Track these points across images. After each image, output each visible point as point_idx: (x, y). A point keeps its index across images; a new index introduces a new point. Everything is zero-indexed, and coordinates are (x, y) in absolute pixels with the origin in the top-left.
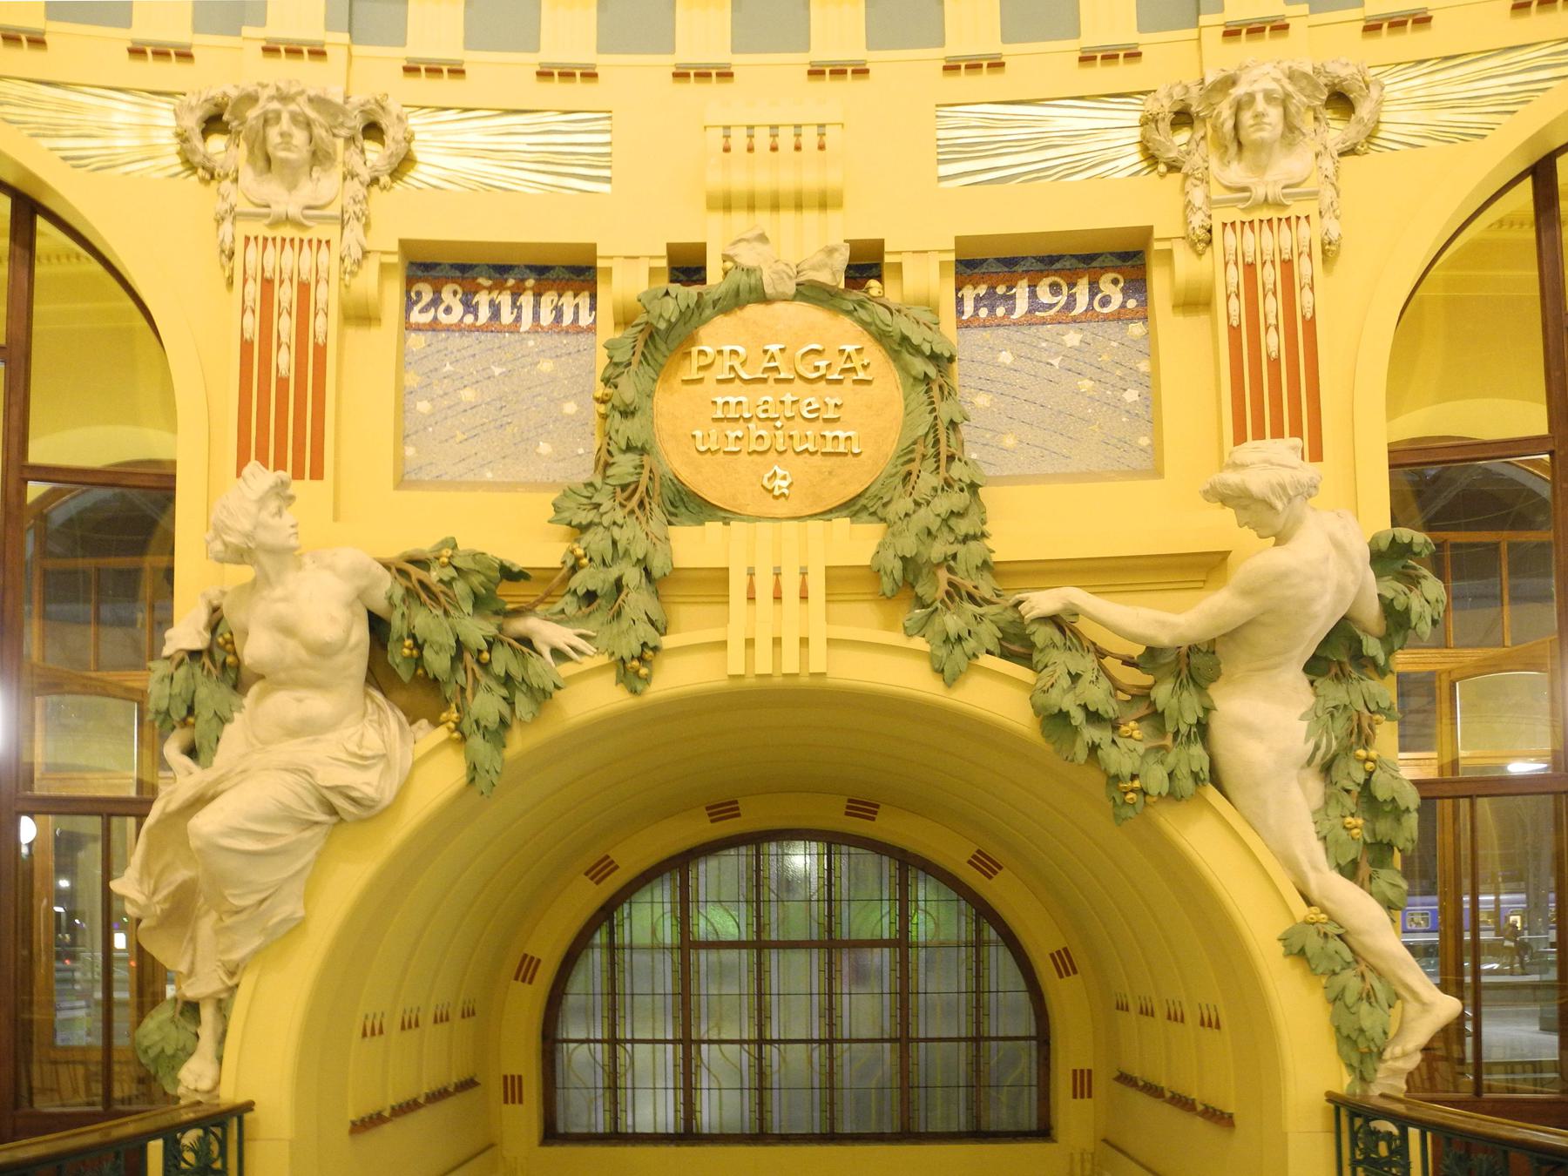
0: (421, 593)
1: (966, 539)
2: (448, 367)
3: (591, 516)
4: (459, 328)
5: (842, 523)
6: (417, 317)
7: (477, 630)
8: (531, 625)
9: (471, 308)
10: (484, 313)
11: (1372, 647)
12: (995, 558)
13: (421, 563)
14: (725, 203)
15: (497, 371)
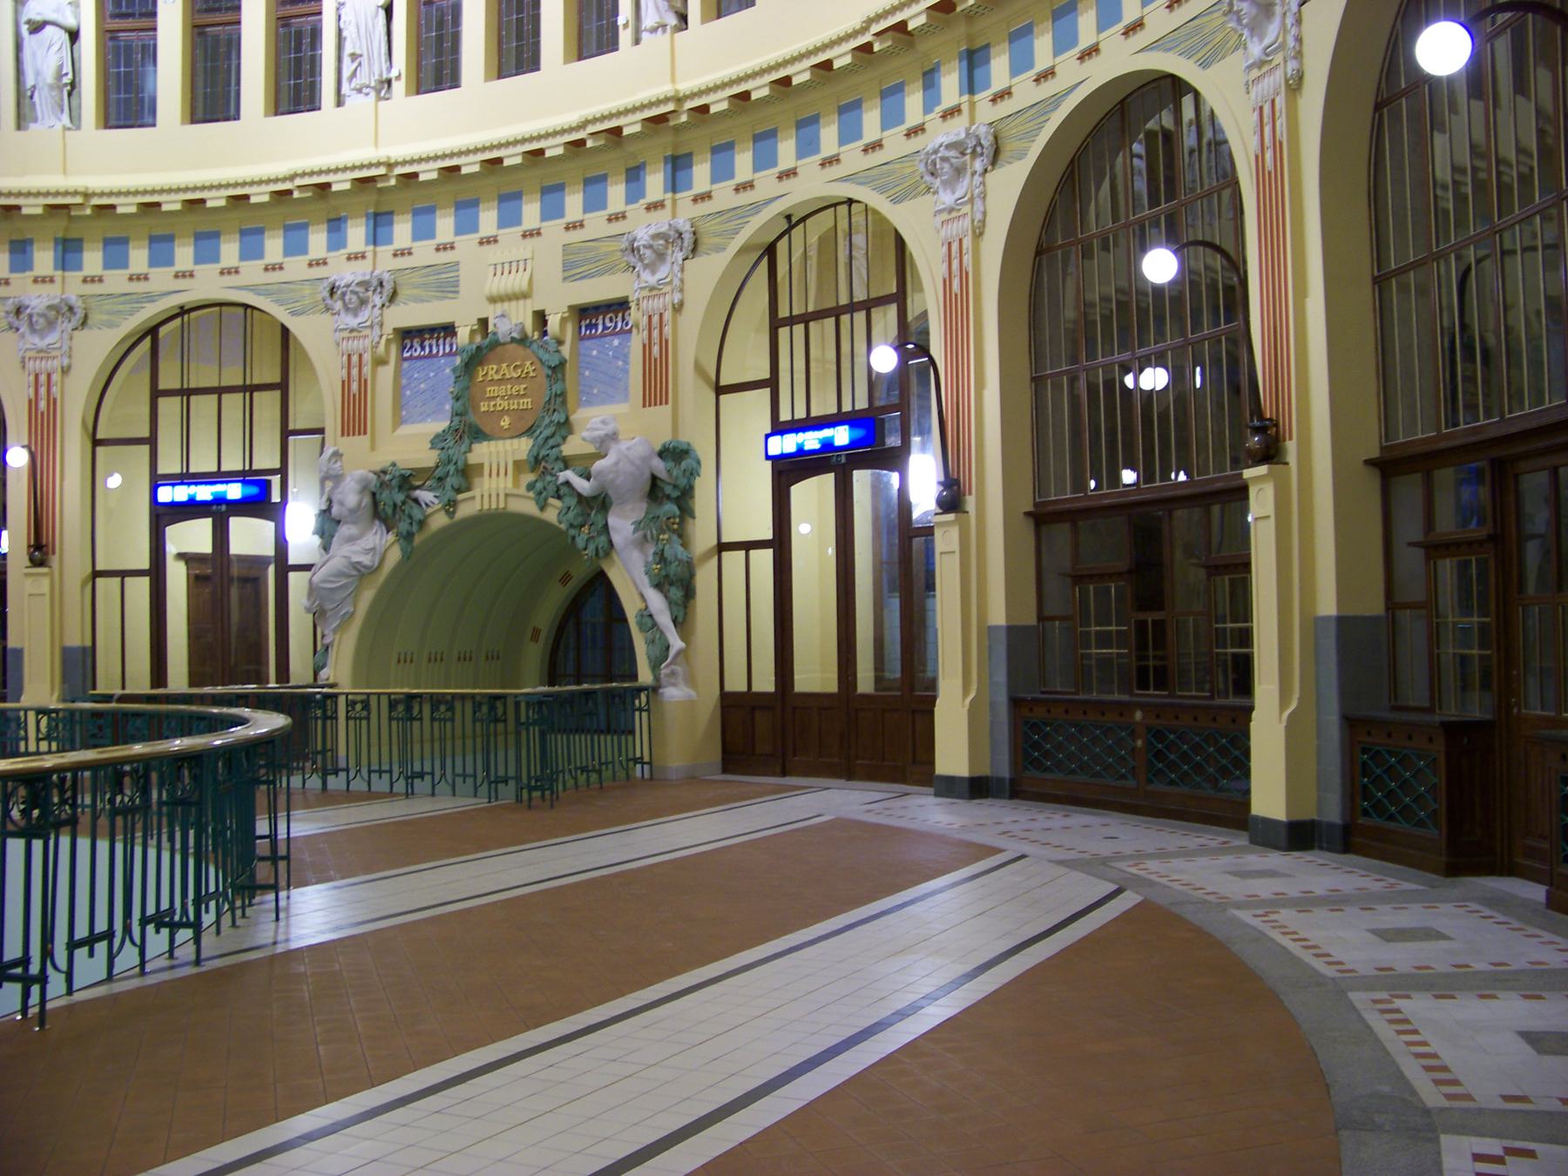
0: (382, 484)
1: (552, 447)
2: (416, 376)
3: (443, 445)
4: (419, 358)
5: (524, 439)
6: (406, 355)
7: (400, 497)
8: (418, 493)
9: (423, 348)
10: (427, 350)
11: (668, 490)
12: (564, 454)
13: (384, 472)
14: (493, 300)
15: (432, 374)
